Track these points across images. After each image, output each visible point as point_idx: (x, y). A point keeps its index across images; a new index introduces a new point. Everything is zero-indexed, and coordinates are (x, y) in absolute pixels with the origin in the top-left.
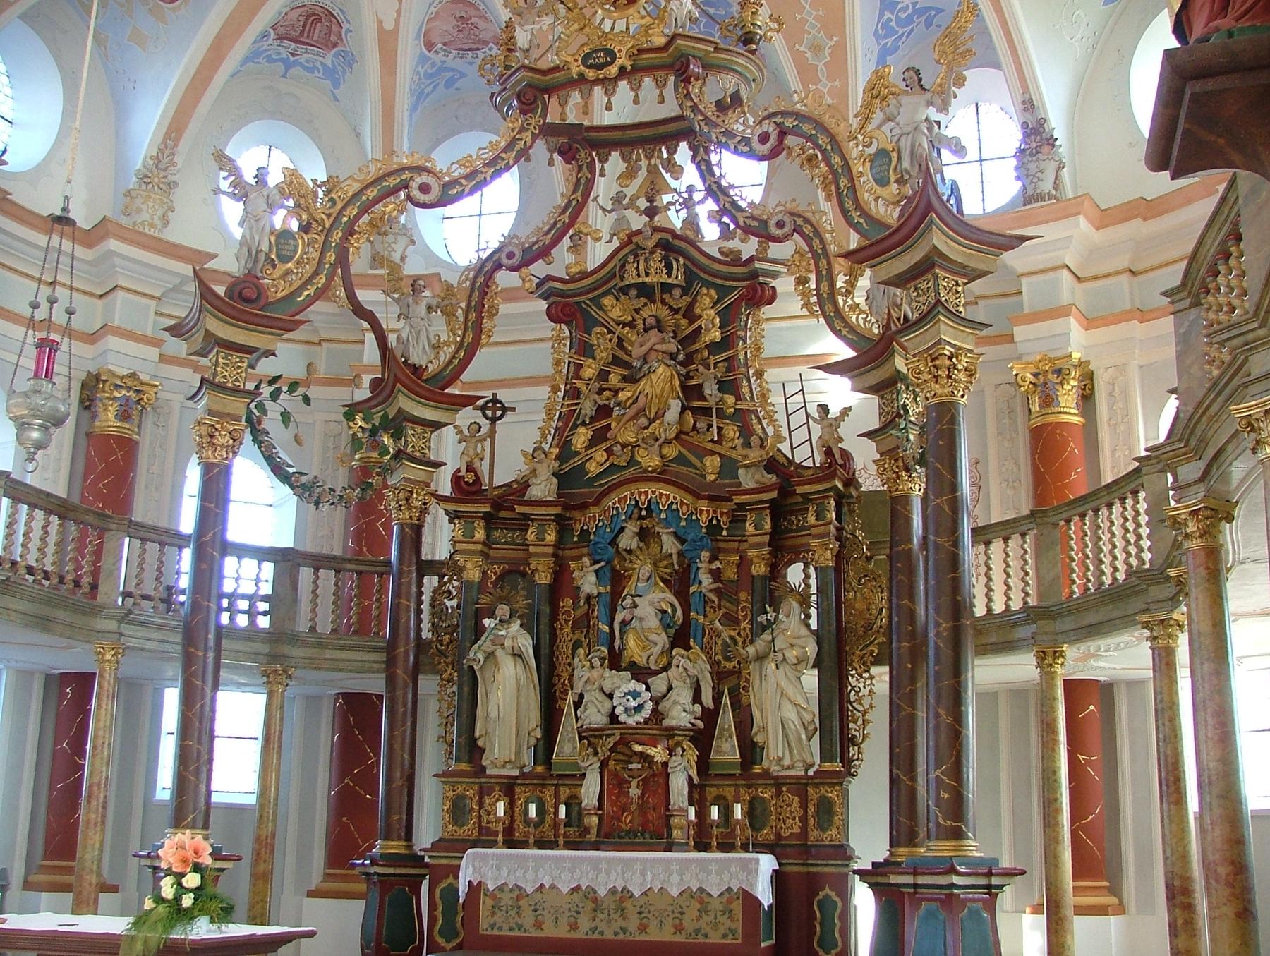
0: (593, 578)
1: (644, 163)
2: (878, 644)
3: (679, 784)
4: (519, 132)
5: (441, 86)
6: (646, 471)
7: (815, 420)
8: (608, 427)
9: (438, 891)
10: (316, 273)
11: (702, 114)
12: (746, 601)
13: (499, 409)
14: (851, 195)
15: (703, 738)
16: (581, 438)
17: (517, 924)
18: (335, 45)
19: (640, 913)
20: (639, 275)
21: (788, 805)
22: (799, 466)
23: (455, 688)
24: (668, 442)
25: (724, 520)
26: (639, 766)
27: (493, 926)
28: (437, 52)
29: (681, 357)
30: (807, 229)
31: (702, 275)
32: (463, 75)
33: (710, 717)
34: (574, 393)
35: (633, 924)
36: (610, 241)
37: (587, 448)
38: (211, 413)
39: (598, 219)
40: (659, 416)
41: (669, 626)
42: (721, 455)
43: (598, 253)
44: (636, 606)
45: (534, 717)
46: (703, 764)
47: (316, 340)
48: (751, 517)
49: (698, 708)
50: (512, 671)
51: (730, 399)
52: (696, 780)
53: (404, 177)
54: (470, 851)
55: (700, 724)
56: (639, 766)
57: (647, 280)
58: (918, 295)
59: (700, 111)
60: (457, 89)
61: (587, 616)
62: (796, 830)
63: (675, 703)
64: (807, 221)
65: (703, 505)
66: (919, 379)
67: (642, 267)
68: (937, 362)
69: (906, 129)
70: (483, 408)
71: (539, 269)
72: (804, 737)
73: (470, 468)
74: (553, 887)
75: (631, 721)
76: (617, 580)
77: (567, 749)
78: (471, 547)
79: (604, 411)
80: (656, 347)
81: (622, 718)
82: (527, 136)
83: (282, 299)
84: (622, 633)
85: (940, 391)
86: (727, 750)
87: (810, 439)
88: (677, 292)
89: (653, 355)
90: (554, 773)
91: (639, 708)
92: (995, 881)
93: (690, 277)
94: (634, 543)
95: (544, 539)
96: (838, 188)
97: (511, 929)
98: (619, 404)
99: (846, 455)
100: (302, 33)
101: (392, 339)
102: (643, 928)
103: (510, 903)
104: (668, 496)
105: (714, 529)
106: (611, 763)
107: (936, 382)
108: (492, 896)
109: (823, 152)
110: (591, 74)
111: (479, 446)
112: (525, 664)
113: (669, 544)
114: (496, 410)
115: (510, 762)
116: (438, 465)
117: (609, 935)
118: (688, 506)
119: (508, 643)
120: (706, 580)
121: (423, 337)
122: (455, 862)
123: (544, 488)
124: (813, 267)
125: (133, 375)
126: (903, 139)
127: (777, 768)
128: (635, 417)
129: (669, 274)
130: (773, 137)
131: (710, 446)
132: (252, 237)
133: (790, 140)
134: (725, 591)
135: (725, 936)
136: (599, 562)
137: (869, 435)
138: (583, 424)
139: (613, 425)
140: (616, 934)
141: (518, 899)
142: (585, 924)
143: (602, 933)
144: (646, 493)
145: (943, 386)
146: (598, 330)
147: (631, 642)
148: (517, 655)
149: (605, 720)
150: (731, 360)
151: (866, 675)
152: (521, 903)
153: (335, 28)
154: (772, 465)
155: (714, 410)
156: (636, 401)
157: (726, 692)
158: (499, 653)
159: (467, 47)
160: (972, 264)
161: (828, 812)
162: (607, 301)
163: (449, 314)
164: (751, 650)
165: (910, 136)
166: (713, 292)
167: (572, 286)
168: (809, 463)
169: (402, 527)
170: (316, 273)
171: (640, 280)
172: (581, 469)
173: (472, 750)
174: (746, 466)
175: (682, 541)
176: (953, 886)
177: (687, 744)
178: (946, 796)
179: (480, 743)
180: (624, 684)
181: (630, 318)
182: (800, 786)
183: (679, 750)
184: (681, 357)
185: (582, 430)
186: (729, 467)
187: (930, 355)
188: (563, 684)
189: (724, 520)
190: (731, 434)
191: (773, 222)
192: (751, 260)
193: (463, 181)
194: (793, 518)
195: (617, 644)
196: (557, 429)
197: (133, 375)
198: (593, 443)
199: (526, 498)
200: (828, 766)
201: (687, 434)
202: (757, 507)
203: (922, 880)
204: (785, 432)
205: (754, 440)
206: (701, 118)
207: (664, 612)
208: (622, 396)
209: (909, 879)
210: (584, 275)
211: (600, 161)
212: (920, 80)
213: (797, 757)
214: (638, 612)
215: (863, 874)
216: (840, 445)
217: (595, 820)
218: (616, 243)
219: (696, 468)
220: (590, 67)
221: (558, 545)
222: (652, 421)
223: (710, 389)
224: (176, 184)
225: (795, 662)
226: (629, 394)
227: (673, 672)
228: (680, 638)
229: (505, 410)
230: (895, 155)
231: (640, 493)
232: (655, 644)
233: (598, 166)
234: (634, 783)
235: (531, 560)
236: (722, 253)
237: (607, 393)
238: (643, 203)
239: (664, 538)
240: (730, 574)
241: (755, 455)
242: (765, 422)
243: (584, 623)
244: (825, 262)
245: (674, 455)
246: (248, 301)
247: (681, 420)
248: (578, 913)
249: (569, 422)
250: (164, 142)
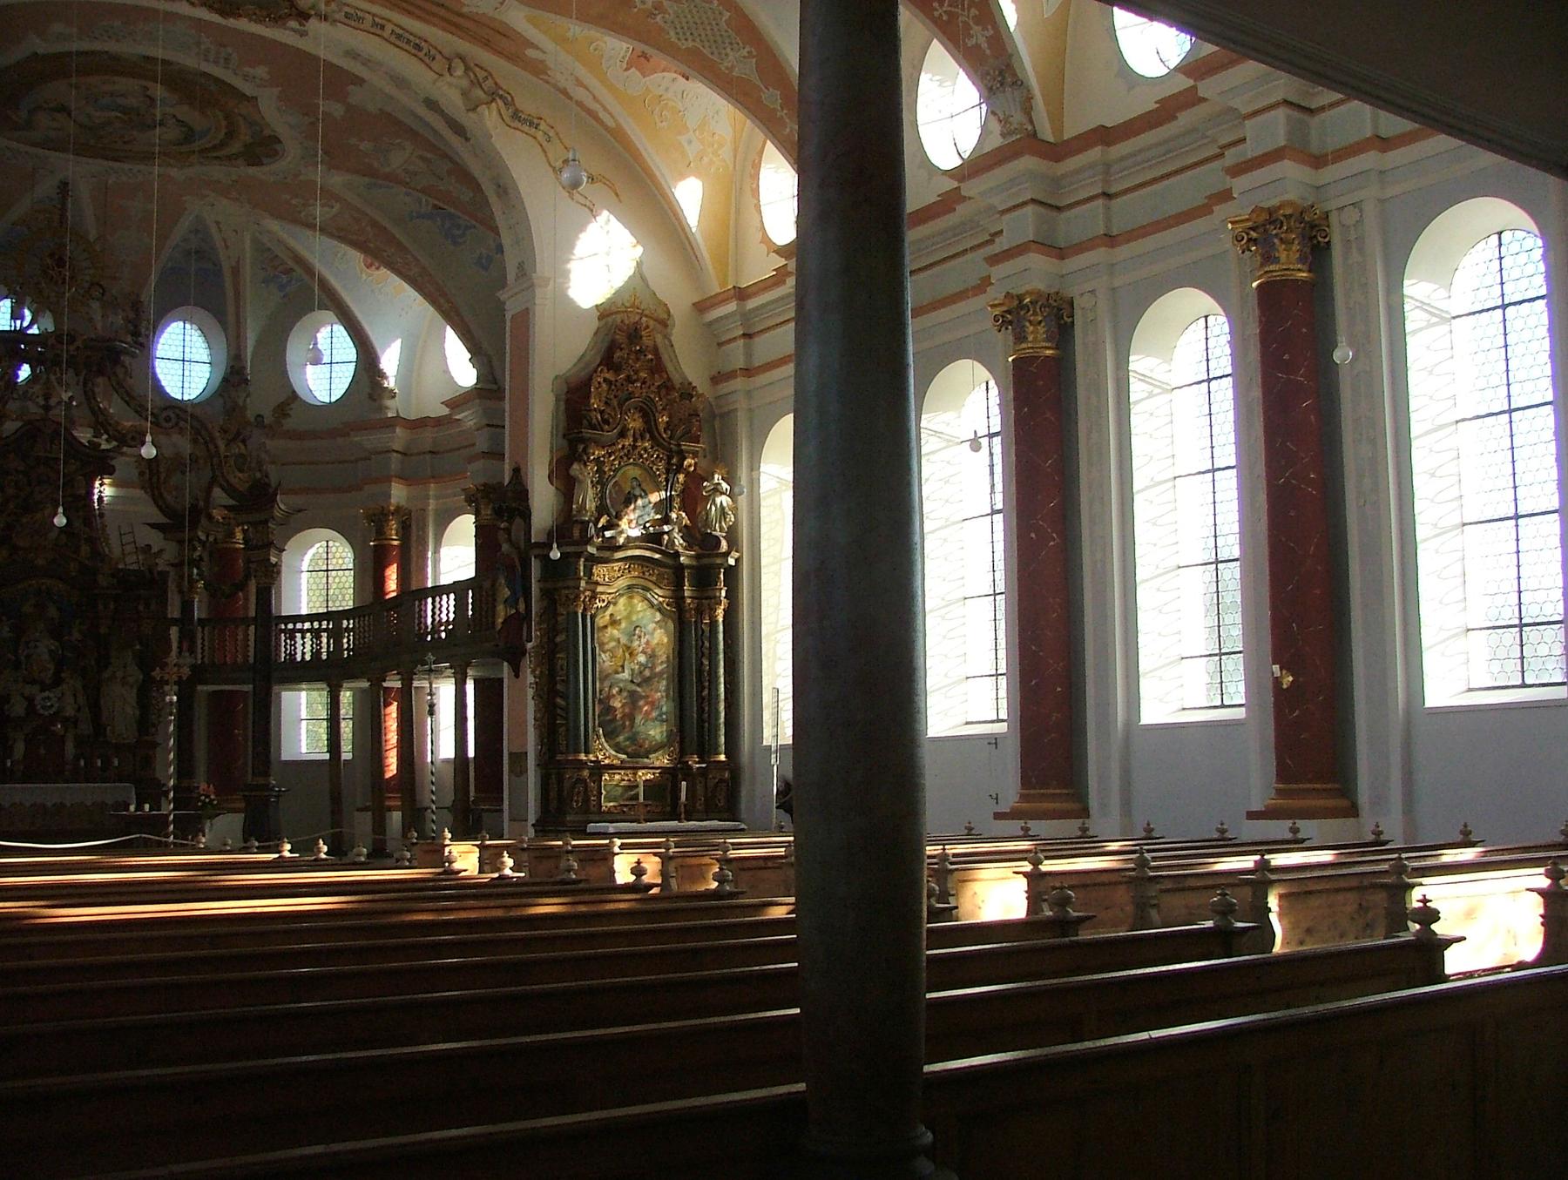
3: (70, 749)
44: (36, 647)
74: (21, 804)
86: (85, 728)
91: (52, 706)
113: (52, 611)
120: (76, 635)
130: (174, 421)
146: (10, 477)
161: (148, 762)
166: (78, 463)
191: (130, 436)
217: (22, 767)
218: (19, 424)
227: (65, 686)
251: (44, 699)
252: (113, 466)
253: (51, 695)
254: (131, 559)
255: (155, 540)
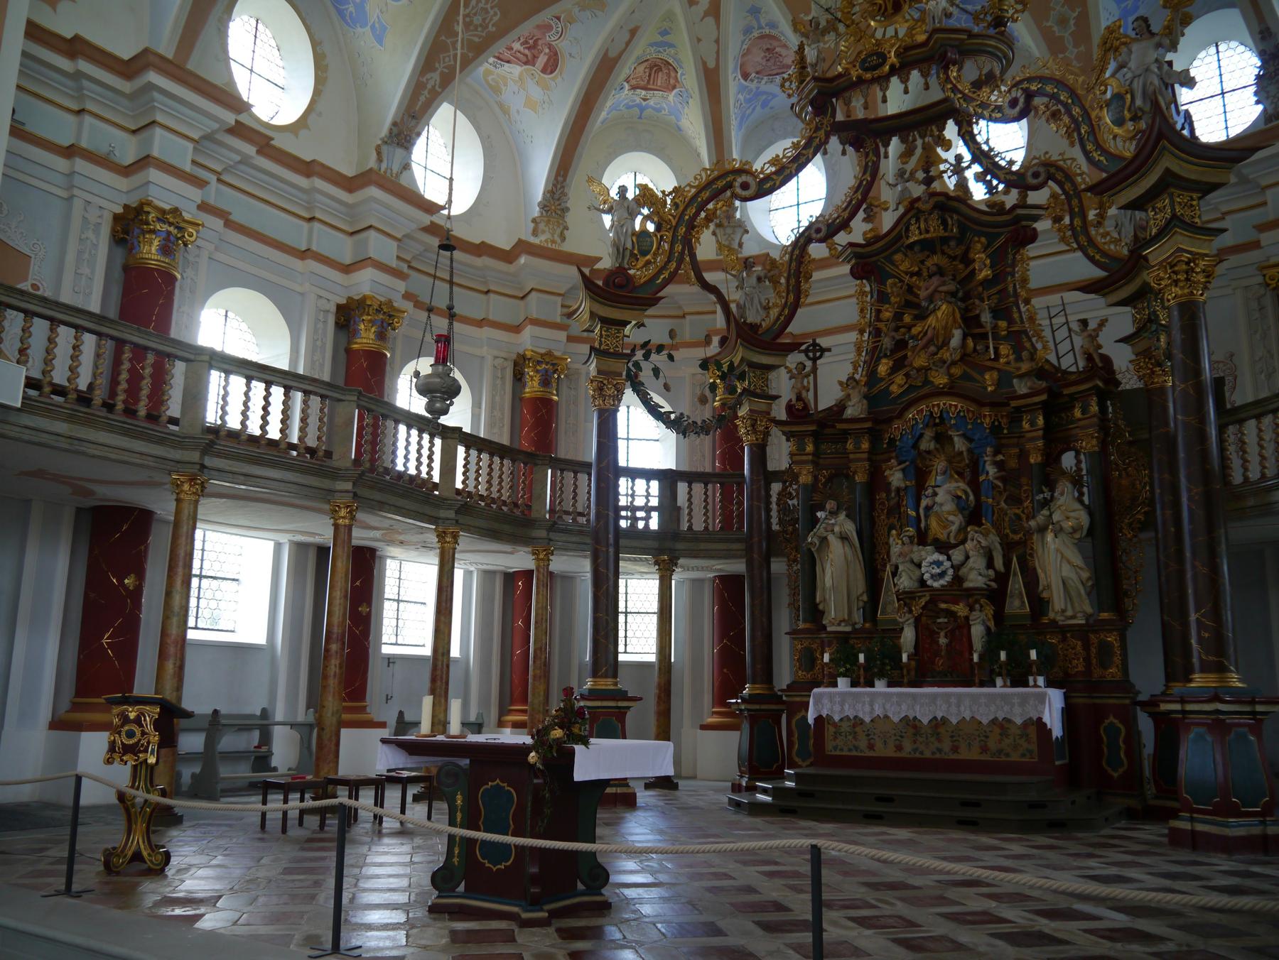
0: (899, 475)
1: (919, 142)
2: (1145, 513)
3: (977, 631)
4: (815, 132)
5: (758, 108)
6: (938, 387)
7: (1076, 333)
8: (905, 357)
9: (794, 721)
10: (669, 261)
11: (961, 92)
12: (1027, 485)
13: (818, 351)
14: (1091, 138)
15: (996, 595)
16: (883, 369)
17: (855, 746)
18: (674, 87)
19: (952, 737)
20: (921, 233)
21: (1073, 649)
22: (1065, 372)
23: (799, 566)
24: (954, 363)
25: (1004, 421)
26: (946, 620)
27: (835, 748)
28: (752, 81)
29: (960, 294)
30: (1059, 176)
31: (975, 227)
32: (774, 96)
33: (1002, 579)
34: (877, 333)
35: (946, 745)
36: (897, 209)
37: (890, 375)
38: (599, 372)
39: (887, 193)
40: (946, 343)
41: (964, 509)
42: (999, 370)
43: (887, 220)
45: (860, 586)
46: (999, 617)
47: (681, 313)
48: (1026, 417)
49: (991, 572)
50: (842, 551)
51: (1003, 324)
52: (993, 628)
53: (728, 179)
54: (815, 690)
55: (994, 585)
56: (946, 620)
57: (927, 236)
58: (1156, 214)
59: (958, 90)
60: (771, 108)
61: (899, 505)
62: (1081, 668)
63: (972, 569)
64: (1059, 169)
65: (986, 411)
66: (1159, 285)
67: (922, 226)
68: (1176, 268)
69: (1138, 72)
70: (806, 352)
71: (842, 238)
72: (1082, 591)
73: (799, 398)
75: (936, 585)
76: (920, 477)
77: (890, 609)
78: (804, 458)
79: (901, 345)
80: (941, 289)
81: (929, 582)
82: (822, 133)
83: (645, 283)
84: (927, 517)
85: (1180, 292)
87: (1073, 349)
88: (952, 243)
89: (937, 296)
90: (879, 628)
91: (942, 575)
92: (1259, 708)
93: (963, 229)
94: (932, 446)
95: (860, 448)
96: (1079, 134)
97: (850, 750)
98: (912, 337)
99: (1107, 360)
100: (649, 81)
101: (733, 307)
102: (955, 749)
103: (848, 729)
104: (956, 406)
105: (995, 429)
106: (924, 619)
107: (1176, 286)
108: (835, 725)
109: (1065, 105)
110: (868, 76)
111: (806, 380)
112: (852, 545)
113: (960, 444)
114: (817, 351)
115: (844, 621)
116: (776, 397)
117: (928, 754)
118: (973, 412)
119: (837, 529)
120: (992, 470)
121: (756, 301)
122: (805, 699)
123: (854, 409)
124: (1066, 207)
125: (549, 354)
126: (1136, 81)
127: (1062, 618)
128: (926, 347)
129: (945, 229)
130: (1022, 100)
131: (989, 364)
132: (619, 239)
133: (1038, 101)
134: (1008, 477)
135: (1023, 755)
136: (905, 462)
137: (1124, 340)
138: (885, 356)
139: (909, 354)
140: (933, 753)
141: (854, 726)
142: (908, 746)
143: (922, 753)
144: (938, 405)
145: (1182, 288)
146: (890, 281)
147: (934, 523)
148: (844, 538)
149: (916, 584)
150: (1004, 290)
151: (1135, 540)
152: (857, 729)
153: (673, 74)
154: (1045, 372)
155: (990, 334)
156: (926, 333)
157: (1015, 559)
158: (831, 538)
159: (775, 72)
160: (1205, 179)
162: (898, 257)
163: (775, 282)
164: (1032, 523)
165: (1142, 78)
166: (983, 239)
167: (869, 249)
168: (1073, 369)
169: (751, 446)
170: (669, 261)
171: (922, 237)
172: (886, 391)
173: (815, 614)
174: (1021, 377)
175: (970, 440)
176: (1218, 712)
177: (983, 601)
178: (1207, 635)
179: (821, 607)
180: (930, 556)
181: (917, 269)
182: (1083, 632)
183: (977, 606)
184: (960, 294)
185: (884, 361)
186: (1005, 379)
187: (1169, 263)
188: (883, 559)
189: (1004, 421)
190: (1006, 352)
191: (1030, 173)
192: (1014, 207)
193: (774, 177)
194: (1063, 415)
195: (923, 525)
196: (865, 362)
197: (549, 354)
198: (894, 370)
199: (844, 417)
200: (1105, 615)
201: (969, 355)
202: (1030, 409)
203: (1189, 707)
204: (1051, 344)
205: (1025, 354)
206: (960, 96)
207: (959, 497)
208: (914, 331)
209: (1177, 707)
210: (878, 238)
211: (884, 146)
212: (1148, 26)
213: (1078, 609)
214: (938, 499)
215: (1143, 705)
216: (1100, 351)
218: (901, 210)
219: (979, 382)
220: (866, 70)
221: (872, 452)
222: (939, 348)
223: (986, 318)
224: (568, 209)
225: (1071, 530)
226: (920, 329)
227: (969, 545)
228: (974, 516)
229: (823, 350)
230: (1129, 96)
231: (933, 406)
232: (953, 523)
233: (882, 150)
234: (942, 634)
235: (851, 465)
236: (988, 206)
237: (902, 330)
238: (920, 175)
239: (956, 439)
240: (1013, 463)
241: (1025, 367)
242: (1034, 339)
243: (896, 511)
244: (1076, 201)
245: (959, 373)
246: (621, 286)
247: (964, 345)
248: (902, 737)
249: (875, 355)
250: (556, 179)
251: (931, 563)
252: (1035, 229)
253: (942, 558)
254: (1064, 347)
255: (1094, 307)
